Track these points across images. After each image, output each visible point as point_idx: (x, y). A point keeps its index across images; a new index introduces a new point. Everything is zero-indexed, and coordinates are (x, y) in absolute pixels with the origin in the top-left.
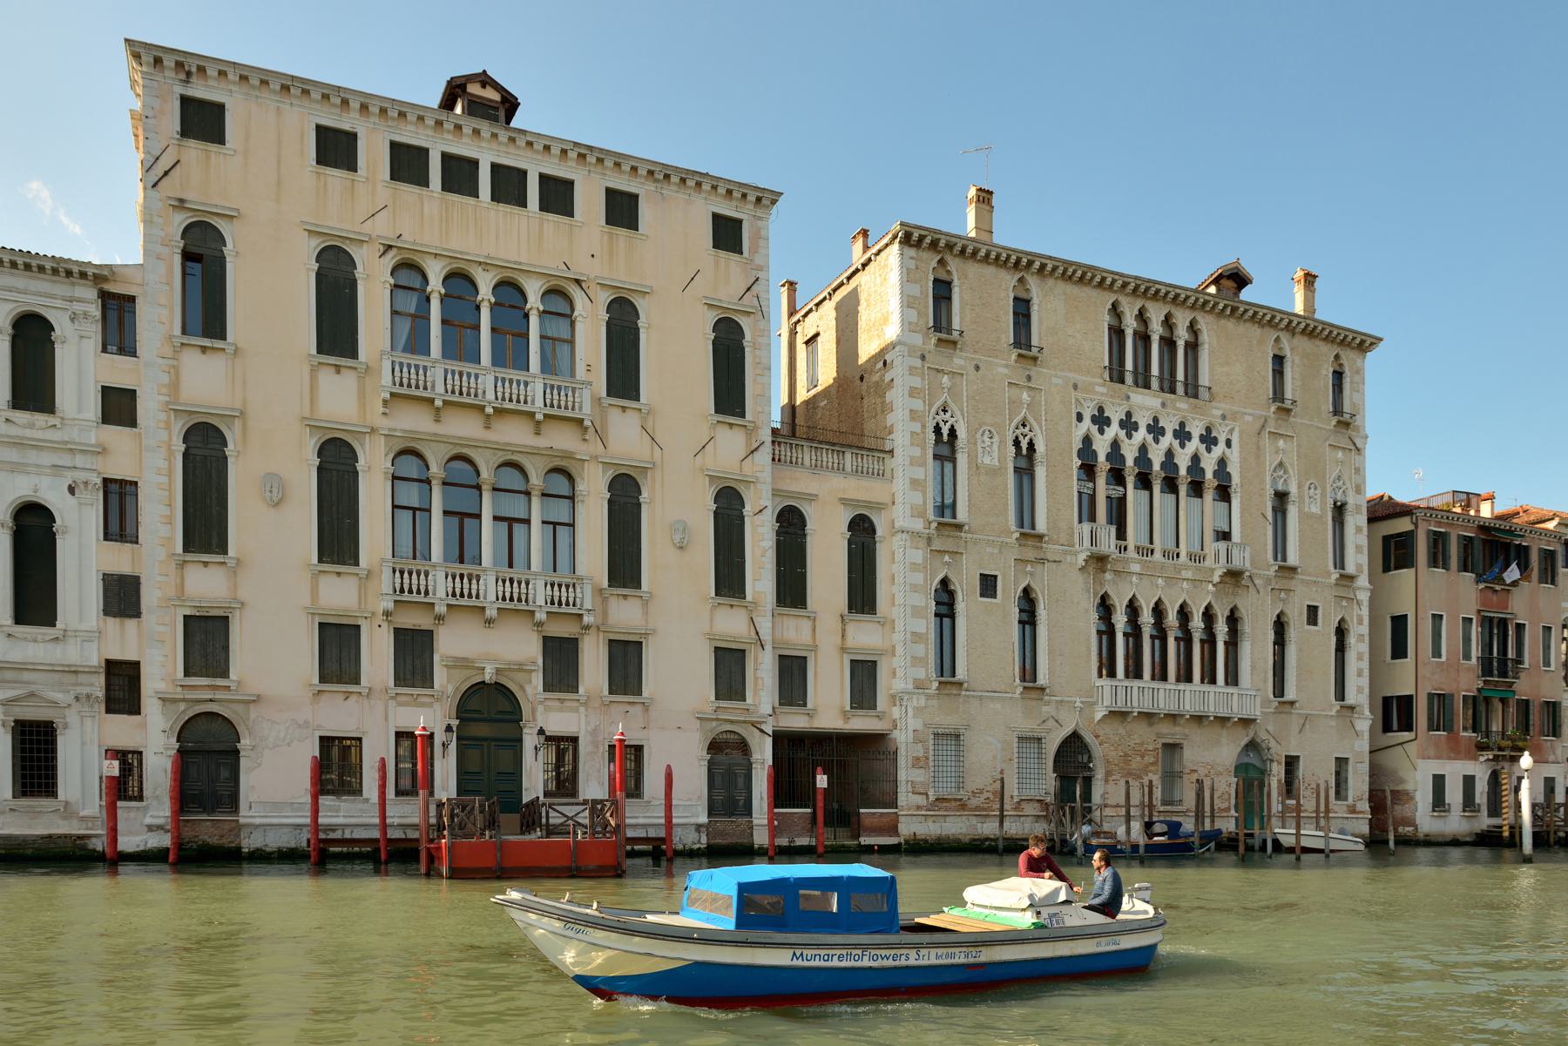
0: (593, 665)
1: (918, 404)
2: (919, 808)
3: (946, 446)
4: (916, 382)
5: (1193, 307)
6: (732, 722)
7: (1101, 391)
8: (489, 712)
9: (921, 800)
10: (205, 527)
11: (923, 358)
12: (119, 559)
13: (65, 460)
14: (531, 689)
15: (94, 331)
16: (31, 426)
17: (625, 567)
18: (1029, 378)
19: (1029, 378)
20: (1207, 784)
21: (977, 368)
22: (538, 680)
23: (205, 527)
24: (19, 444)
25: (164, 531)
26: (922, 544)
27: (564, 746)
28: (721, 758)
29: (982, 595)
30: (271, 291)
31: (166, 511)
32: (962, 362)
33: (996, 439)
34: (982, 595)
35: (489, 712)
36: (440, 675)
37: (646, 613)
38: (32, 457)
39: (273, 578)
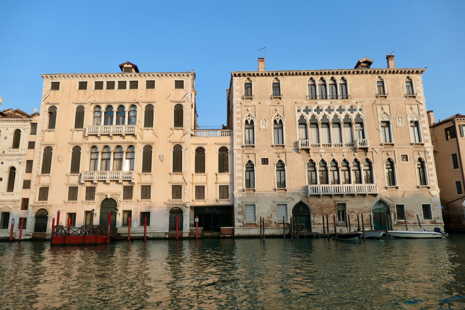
0: (137, 192)
1: (239, 116)
2: (240, 226)
3: (250, 125)
4: (239, 110)
5: (341, 73)
6: (176, 205)
7: (307, 103)
8: (109, 205)
9: (242, 224)
10: (46, 168)
11: (241, 104)
12: (27, 177)
13: (19, 157)
14: (120, 199)
15: (29, 131)
16: (14, 151)
17: (147, 167)
18: (278, 103)
19: (278, 103)
20: (360, 215)
21: (260, 103)
22: (122, 196)
23: (46, 168)
24: (11, 155)
25: (37, 170)
26: (241, 152)
27: (129, 213)
28: (173, 215)
29: (262, 164)
30: (66, 118)
31: (38, 165)
32: (255, 103)
33: (267, 121)
34: (262, 164)
35: (109, 205)
36: (96, 197)
37: (152, 178)
38: (13, 157)
39: (60, 178)
